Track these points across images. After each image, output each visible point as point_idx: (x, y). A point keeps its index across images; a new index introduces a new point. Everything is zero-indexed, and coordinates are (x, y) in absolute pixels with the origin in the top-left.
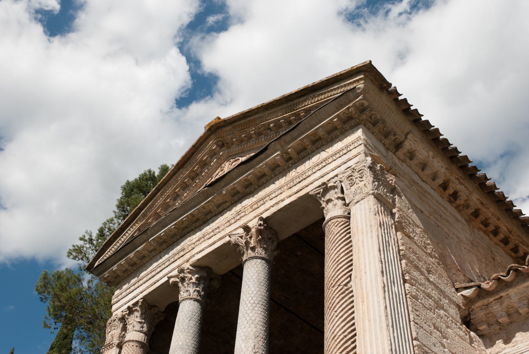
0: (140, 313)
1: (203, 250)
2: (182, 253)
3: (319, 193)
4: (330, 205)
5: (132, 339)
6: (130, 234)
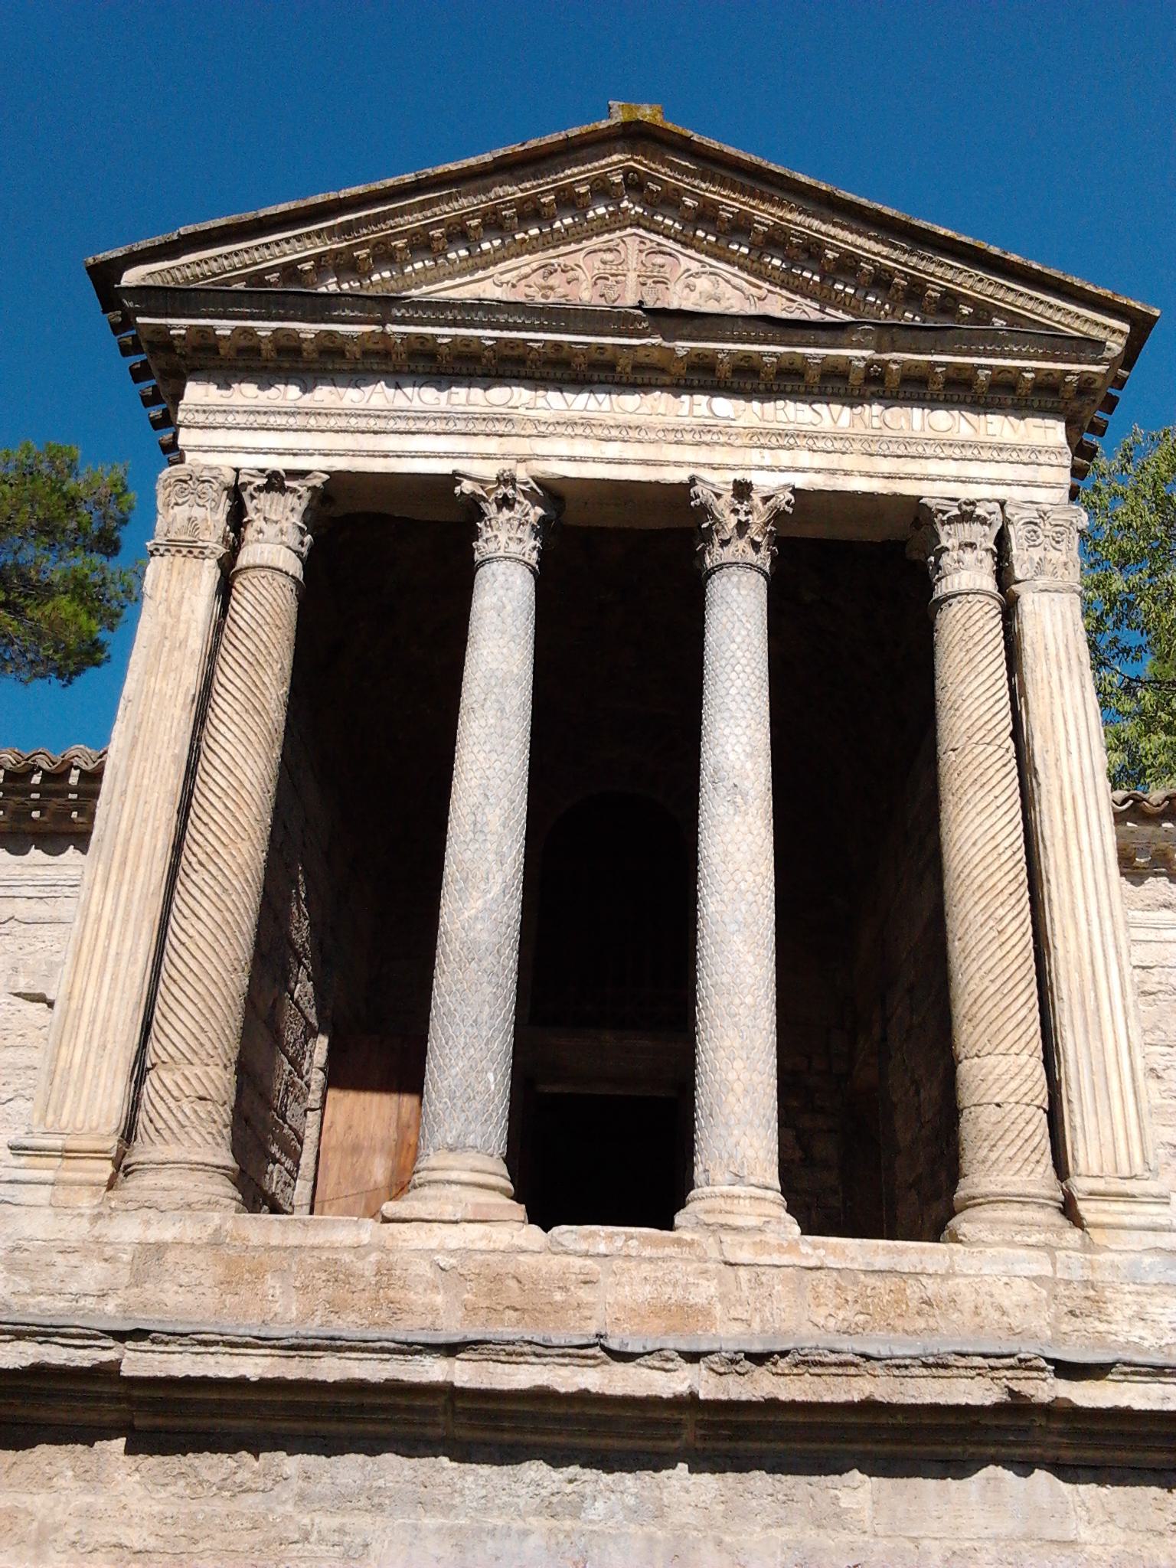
0: (304, 503)
1: (583, 460)
2: (500, 428)
3: (944, 512)
4: (969, 556)
5: (280, 565)
6: (285, 255)
